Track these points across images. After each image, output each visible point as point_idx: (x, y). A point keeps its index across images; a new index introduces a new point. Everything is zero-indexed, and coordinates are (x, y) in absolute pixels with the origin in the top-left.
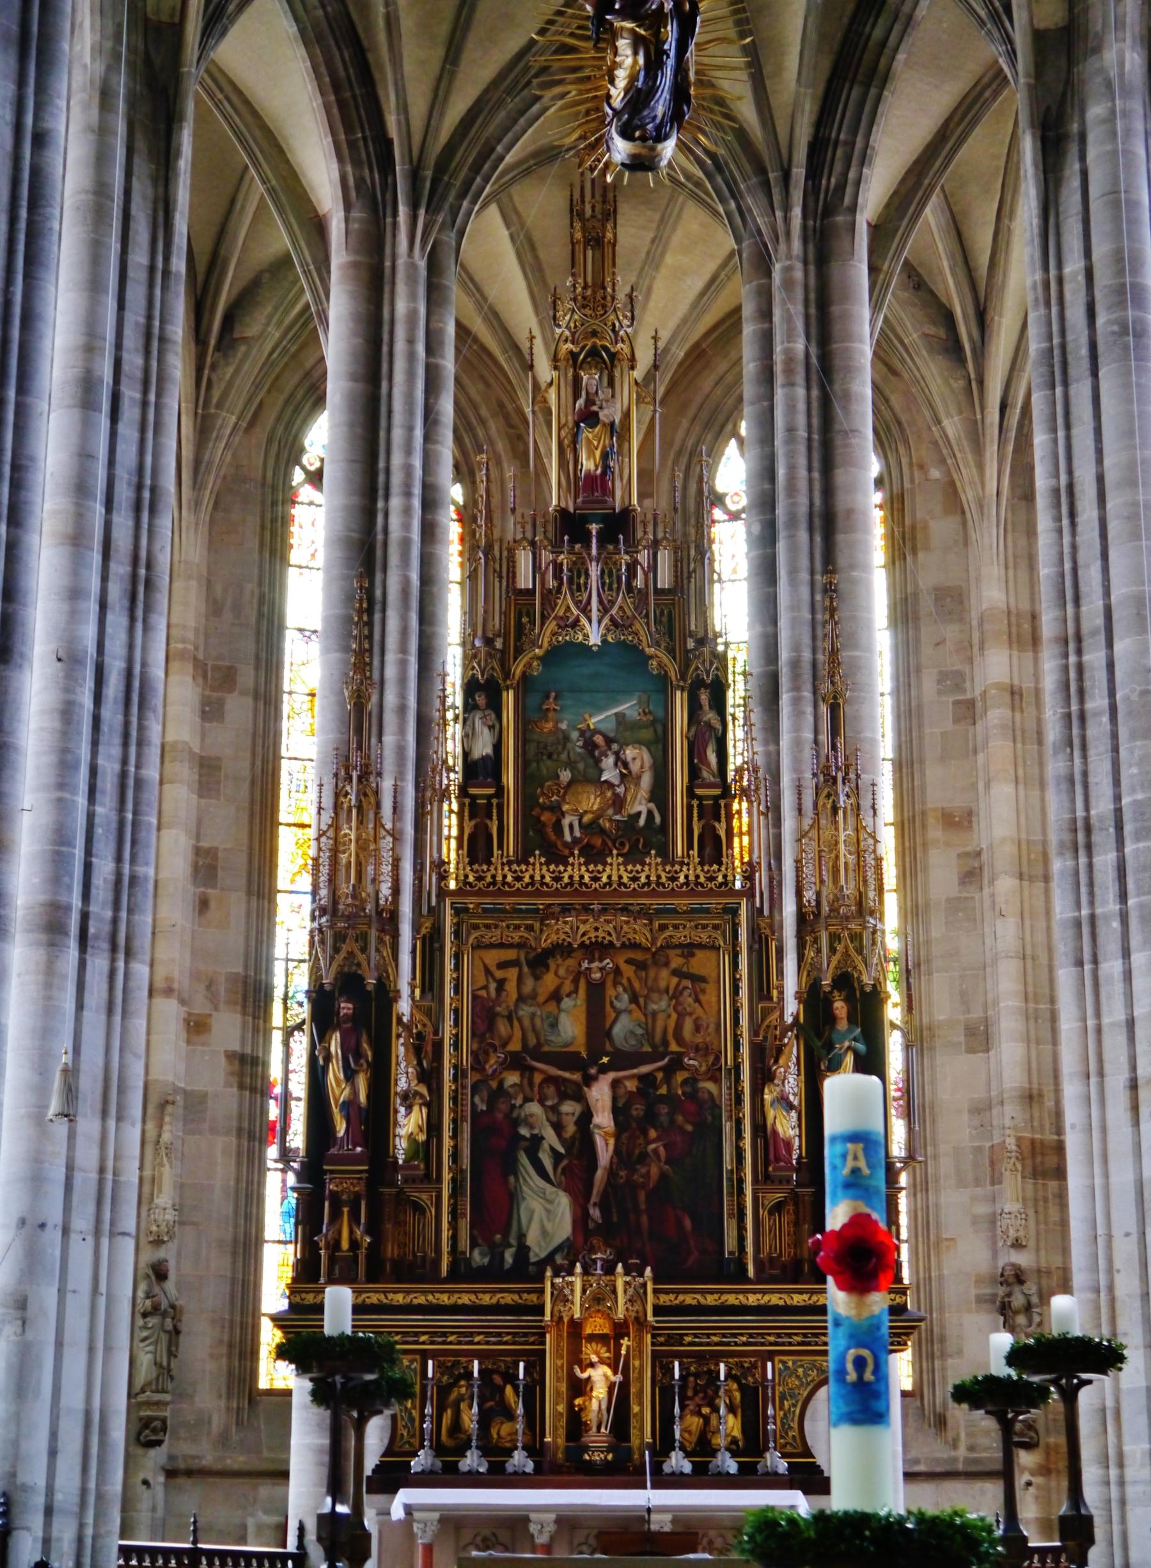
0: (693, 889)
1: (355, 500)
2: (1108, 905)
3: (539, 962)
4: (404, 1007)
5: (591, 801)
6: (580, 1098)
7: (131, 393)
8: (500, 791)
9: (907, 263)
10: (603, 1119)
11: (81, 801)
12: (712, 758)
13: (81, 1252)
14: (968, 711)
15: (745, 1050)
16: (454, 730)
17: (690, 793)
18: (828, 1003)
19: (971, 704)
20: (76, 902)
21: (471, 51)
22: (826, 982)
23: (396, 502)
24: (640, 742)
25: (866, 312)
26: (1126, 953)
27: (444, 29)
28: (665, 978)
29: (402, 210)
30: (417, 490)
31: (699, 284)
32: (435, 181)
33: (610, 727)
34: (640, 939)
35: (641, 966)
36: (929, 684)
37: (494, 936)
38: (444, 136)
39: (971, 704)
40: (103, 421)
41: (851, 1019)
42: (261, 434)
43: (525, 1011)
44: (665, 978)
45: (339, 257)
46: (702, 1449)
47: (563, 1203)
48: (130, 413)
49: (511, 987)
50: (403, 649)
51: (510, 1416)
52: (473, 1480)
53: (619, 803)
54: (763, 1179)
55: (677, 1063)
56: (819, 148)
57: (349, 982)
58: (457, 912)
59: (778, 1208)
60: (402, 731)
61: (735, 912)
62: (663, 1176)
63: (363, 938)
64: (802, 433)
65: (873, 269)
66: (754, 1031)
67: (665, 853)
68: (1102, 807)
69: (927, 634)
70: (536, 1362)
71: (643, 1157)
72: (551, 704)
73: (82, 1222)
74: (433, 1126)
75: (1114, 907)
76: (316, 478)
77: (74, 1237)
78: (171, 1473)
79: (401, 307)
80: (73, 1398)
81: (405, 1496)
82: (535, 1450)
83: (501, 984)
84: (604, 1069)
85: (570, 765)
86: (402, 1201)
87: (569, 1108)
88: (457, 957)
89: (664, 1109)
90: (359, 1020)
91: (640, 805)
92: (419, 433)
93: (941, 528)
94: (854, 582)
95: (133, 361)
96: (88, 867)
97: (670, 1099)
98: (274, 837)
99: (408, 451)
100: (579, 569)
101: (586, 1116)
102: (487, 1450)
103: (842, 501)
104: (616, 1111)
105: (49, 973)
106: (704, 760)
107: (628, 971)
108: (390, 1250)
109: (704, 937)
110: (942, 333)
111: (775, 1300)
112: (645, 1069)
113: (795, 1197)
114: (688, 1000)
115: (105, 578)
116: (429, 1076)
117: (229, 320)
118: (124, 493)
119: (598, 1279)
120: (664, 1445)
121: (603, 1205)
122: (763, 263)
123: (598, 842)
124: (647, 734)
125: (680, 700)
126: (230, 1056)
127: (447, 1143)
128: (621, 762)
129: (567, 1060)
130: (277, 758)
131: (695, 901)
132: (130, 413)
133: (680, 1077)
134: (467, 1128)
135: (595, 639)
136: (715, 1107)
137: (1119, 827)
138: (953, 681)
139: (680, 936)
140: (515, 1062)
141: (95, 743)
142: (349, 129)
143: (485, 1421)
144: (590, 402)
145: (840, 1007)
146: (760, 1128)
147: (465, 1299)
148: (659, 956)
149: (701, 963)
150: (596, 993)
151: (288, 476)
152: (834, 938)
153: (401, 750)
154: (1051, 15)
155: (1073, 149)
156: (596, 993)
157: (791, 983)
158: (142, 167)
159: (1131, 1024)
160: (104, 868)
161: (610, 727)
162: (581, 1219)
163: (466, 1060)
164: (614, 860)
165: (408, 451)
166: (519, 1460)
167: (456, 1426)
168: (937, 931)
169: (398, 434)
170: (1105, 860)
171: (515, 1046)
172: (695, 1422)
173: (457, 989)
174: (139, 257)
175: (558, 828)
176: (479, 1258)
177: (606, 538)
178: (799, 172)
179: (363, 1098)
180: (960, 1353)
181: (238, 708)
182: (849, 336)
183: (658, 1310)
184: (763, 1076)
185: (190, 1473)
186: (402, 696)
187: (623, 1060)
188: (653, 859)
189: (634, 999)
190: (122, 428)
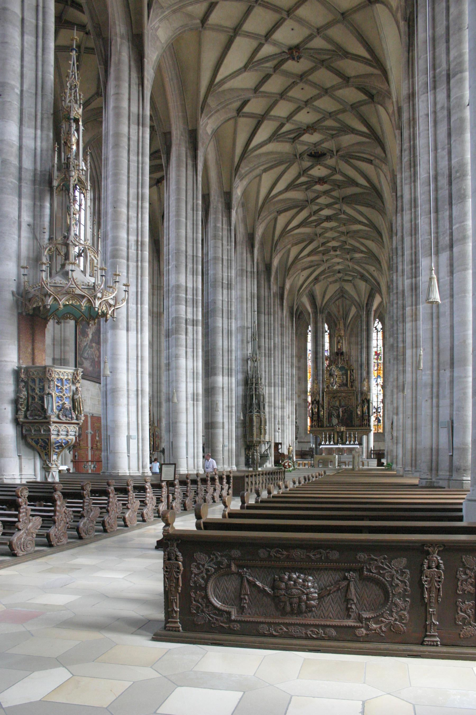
3: (334, 398)
10: (341, 413)
48: (290, 348)
57: (315, 400)
76: (310, 331)
95: (290, 343)
101: (339, 412)
104: (342, 412)
117: (299, 316)
129: (337, 407)
156: (340, 401)
157: (359, 399)
160: (290, 392)
174: (290, 332)
184: (357, 408)
187: (342, 407)
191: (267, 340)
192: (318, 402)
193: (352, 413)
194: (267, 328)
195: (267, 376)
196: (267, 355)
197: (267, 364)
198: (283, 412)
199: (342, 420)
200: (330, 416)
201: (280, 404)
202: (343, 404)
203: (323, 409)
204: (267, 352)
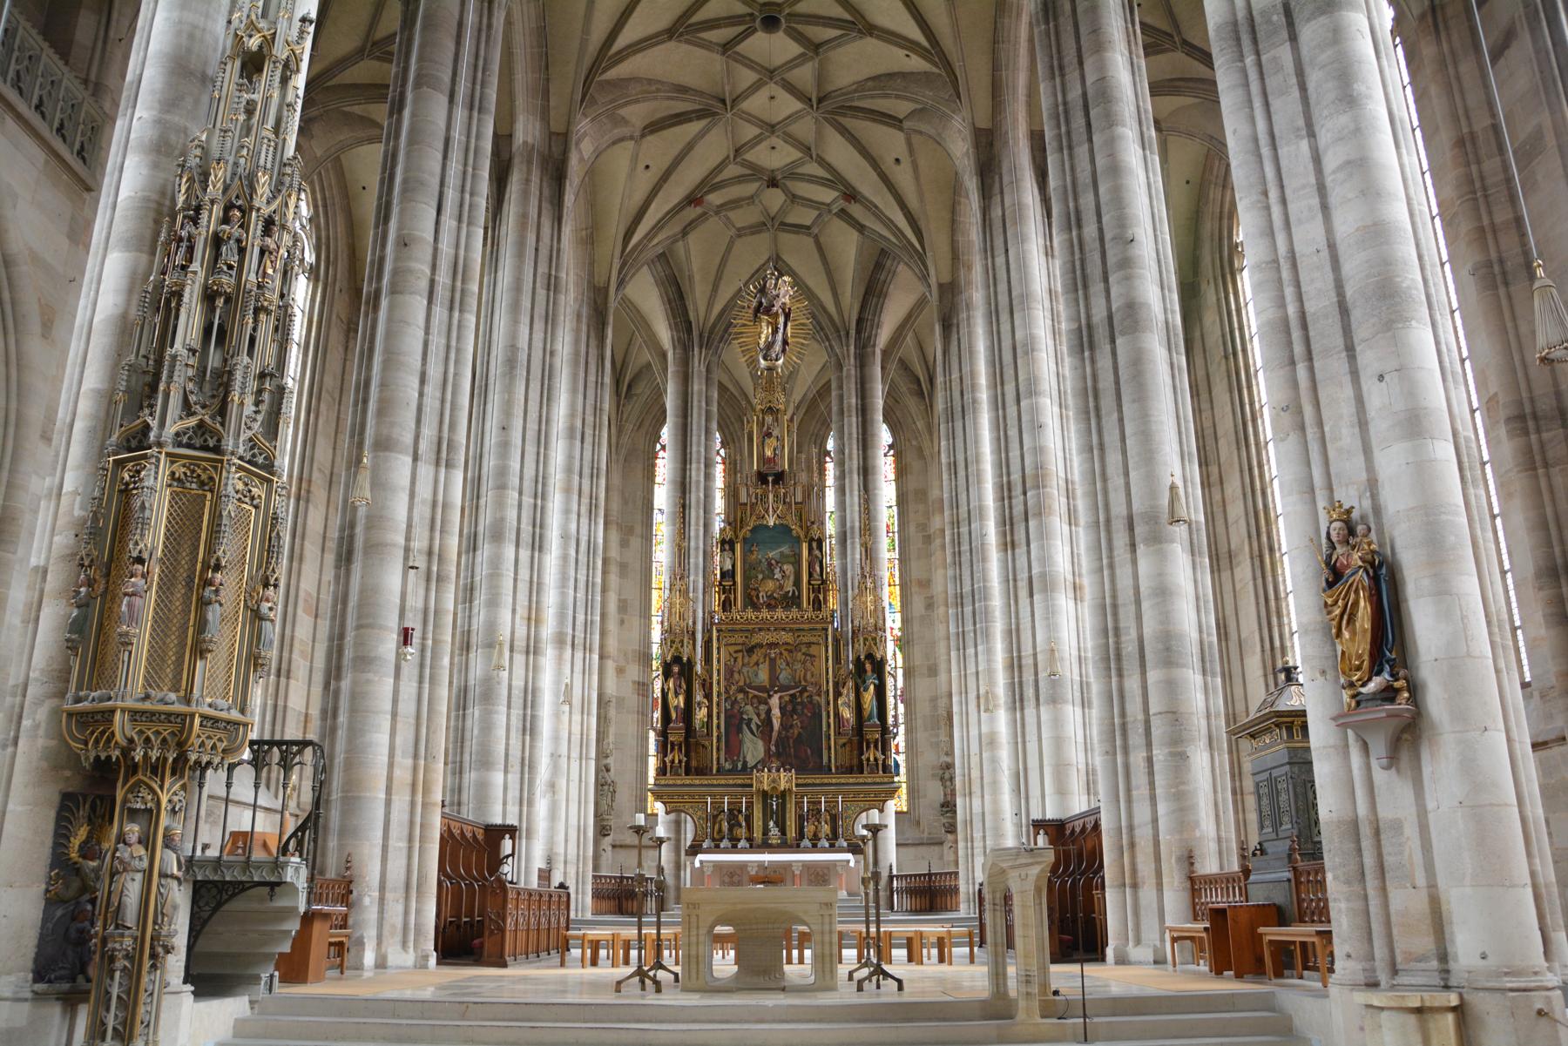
0: (810, 621)
1: (679, 466)
2: (969, 627)
3: (750, 650)
4: (698, 668)
5: (770, 585)
6: (767, 703)
7: (589, 432)
8: (735, 583)
9: (900, 359)
10: (776, 712)
11: (571, 592)
12: (818, 569)
13: (575, 765)
14: (928, 539)
15: (831, 684)
16: (718, 558)
17: (809, 583)
18: (864, 665)
19: (929, 536)
20: (570, 631)
21: (722, 287)
22: (862, 657)
23: (694, 466)
24: (789, 563)
25: (880, 387)
26: (976, 646)
27: (712, 279)
28: (800, 656)
29: (696, 349)
30: (703, 460)
31: (819, 368)
32: (709, 338)
33: (777, 557)
34: (789, 641)
35: (790, 651)
36: (912, 528)
37: (732, 640)
38: (712, 320)
39: (929, 536)
40: (578, 443)
41: (873, 671)
42: (643, 430)
43: (745, 670)
44: (800, 656)
45: (671, 369)
46: (815, 838)
47: (760, 744)
48: (588, 439)
49: (740, 660)
50: (697, 524)
51: (741, 826)
52: (725, 851)
53: (781, 587)
54: (838, 733)
55: (804, 690)
56: (860, 321)
57: (677, 659)
58: (718, 631)
59: (844, 745)
60: (697, 557)
61: (827, 630)
62: (799, 733)
63: (682, 641)
64: (855, 436)
65: (883, 368)
66: (834, 677)
67: (799, 606)
68: (967, 589)
69: (912, 507)
70: (750, 805)
71: (791, 726)
72: (754, 548)
73: (575, 754)
74: (710, 715)
75: (971, 628)
77: (572, 760)
78: (614, 846)
79: (696, 388)
80: (573, 821)
81: (700, 857)
82: (750, 839)
83: (736, 659)
84: (776, 692)
85: (762, 572)
86: (697, 744)
87: (763, 707)
88: (719, 649)
89: (799, 707)
90: (681, 673)
91: (789, 587)
92: (703, 438)
93: (916, 465)
94: (875, 495)
95: (590, 419)
96: (574, 617)
97: (802, 703)
98: (650, 593)
99: (699, 444)
100: (765, 495)
101: (769, 711)
102: (730, 840)
103: (870, 462)
104: (780, 708)
105: (559, 660)
106: (814, 569)
107: (785, 653)
108: (694, 763)
109: (814, 639)
110: (916, 387)
111: (843, 781)
112: (792, 692)
113: (850, 741)
114: (808, 664)
115: (579, 505)
116: (708, 696)
117: (630, 386)
118: (586, 471)
119: (774, 773)
120: (801, 835)
121: (777, 746)
122: (840, 366)
123: (773, 602)
124: (792, 559)
125: (805, 546)
126: (634, 682)
127: (715, 721)
128: (782, 571)
129: (761, 689)
130: (651, 561)
131: (811, 626)
132: (588, 439)
133: (806, 694)
134: (723, 716)
135: (771, 524)
136: (820, 706)
137: (973, 596)
138: (923, 527)
139: (805, 640)
140: (741, 690)
141: (576, 569)
142: (674, 318)
143: (731, 829)
144: (769, 428)
145: (868, 666)
146: (837, 714)
147: (723, 782)
148: (797, 648)
149: (813, 650)
150: (773, 661)
151: (655, 447)
152: (865, 639)
153: (697, 565)
154: (946, 278)
155: (955, 329)
156: (773, 661)
158: (593, 343)
159: (977, 673)
160: (581, 618)
161: (777, 557)
162: (767, 750)
163: (723, 690)
164: (779, 610)
165: (699, 444)
166: (742, 844)
167: (720, 831)
168: (916, 628)
169: (695, 439)
170: (968, 609)
171: (741, 683)
172: (812, 828)
173: (719, 661)
174: (592, 378)
175: (758, 597)
176: (728, 766)
177: (776, 482)
178: (853, 332)
179: (682, 705)
180: (925, 796)
181: (636, 542)
182: (872, 397)
183: (797, 785)
184: (838, 694)
185: (621, 846)
186: (697, 543)
187: (783, 688)
188: (795, 609)
189: (788, 664)
190: (585, 445)
191: (449, 222)
192: (686, 669)
193: (817, 716)
195: (431, 403)
196: (442, 293)
197: (437, 341)
198: (533, 670)
199: (781, 742)
200: (735, 723)
201: (521, 631)
202: (784, 676)
203: (708, 696)
204: (443, 278)
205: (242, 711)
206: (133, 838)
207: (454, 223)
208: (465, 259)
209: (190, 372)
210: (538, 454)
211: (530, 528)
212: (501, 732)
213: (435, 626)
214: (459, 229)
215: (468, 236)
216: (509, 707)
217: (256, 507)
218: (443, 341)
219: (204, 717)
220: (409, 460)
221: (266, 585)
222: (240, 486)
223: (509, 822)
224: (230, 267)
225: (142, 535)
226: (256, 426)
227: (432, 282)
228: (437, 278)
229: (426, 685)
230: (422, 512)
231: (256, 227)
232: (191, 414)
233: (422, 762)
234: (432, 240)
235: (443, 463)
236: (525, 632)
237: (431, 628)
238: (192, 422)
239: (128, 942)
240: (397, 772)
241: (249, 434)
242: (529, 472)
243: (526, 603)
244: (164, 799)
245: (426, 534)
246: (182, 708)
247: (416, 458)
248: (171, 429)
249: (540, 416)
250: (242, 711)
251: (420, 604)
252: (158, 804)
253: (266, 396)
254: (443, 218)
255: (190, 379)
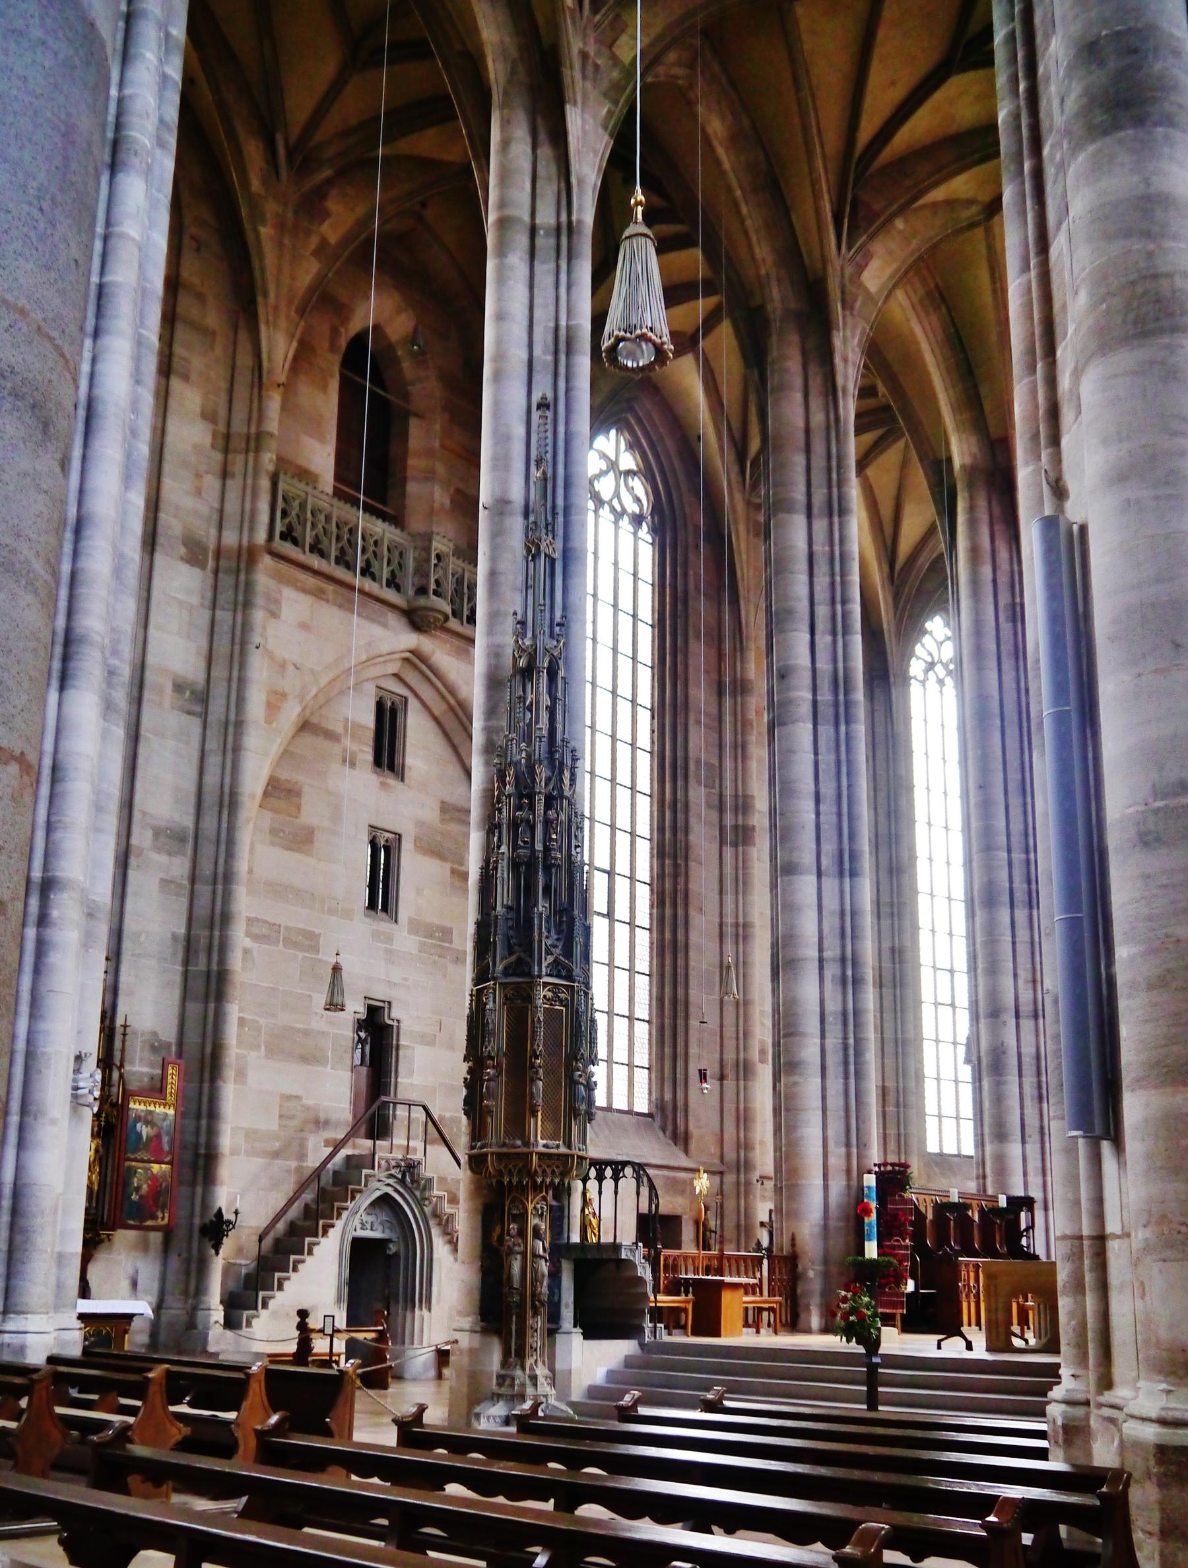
191: (823, 640)
194: (822, 581)
195: (829, 819)
196: (826, 711)
197: (827, 758)
204: (825, 696)
205: (569, 1147)
206: (513, 1232)
207: (829, 638)
208: (845, 669)
209: (510, 923)
210: (1025, 804)
211: (1025, 886)
212: (1014, 1103)
213: (856, 1025)
214: (835, 642)
215: (845, 646)
216: (1020, 1076)
217: (566, 1006)
218: (833, 757)
219: (540, 1155)
220: (813, 879)
221: (577, 1061)
222: (550, 994)
223: (1032, 1194)
224: (525, 842)
225: (489, 1042)
226: (558, 951)
227: (815, 703)
228: (819, 698)
229: (852, 1081)
230: (831, 923)
231: (540, 807)
232: (511, 953)
233: (854, 1150)
234: (808, 663)
235: (847, 873)
236: (1031, 996)
237: (851, 1027)
238: (513, 958)
239: (516, 1298)
240: (832, 1161)
241: (550, 959)
242: (1017, 827)
243: (1029, 966)
244: (530, 1207)
245: (838, 942)
246: (525, 1150)
247: (819, 875)
248: (500, 968)
249: (1022, 763)
250: (569, 1147)
251: (839, 1008)
252: (526, 1210)
253: (564, 926)
254: (817, 637)
255: (511, 928)
